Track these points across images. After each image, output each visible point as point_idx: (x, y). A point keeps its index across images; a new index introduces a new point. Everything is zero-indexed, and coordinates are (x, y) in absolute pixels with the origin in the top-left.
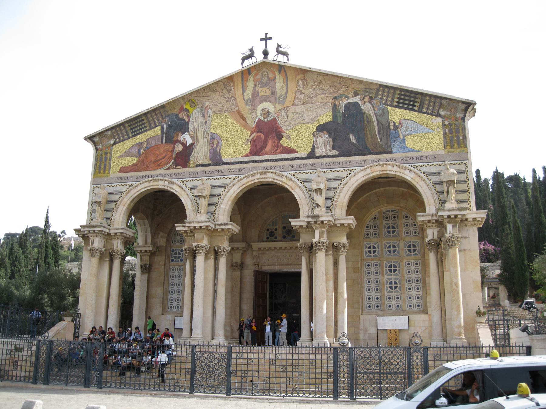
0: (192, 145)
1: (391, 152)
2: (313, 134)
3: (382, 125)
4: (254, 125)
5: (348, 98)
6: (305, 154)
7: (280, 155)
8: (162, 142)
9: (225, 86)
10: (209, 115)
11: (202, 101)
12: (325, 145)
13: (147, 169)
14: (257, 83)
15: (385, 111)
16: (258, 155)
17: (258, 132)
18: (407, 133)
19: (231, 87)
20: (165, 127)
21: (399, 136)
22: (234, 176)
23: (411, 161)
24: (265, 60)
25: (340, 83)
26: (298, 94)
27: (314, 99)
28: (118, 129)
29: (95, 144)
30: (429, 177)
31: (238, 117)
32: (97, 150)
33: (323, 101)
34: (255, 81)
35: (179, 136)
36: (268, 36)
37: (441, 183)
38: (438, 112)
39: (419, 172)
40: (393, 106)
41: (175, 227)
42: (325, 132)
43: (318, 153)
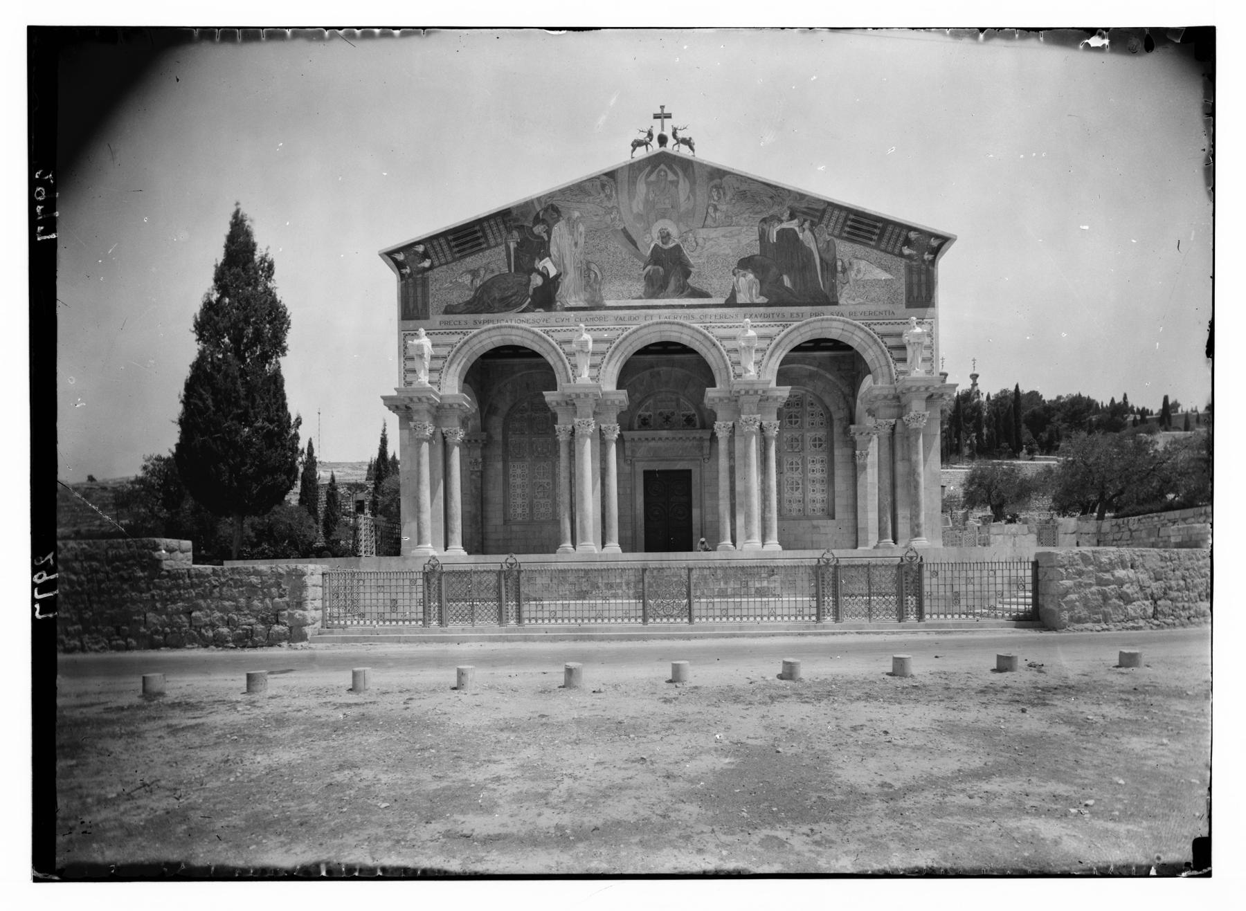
0: (557, 276)
1: (836, 303)
2: (733, 271)
3: (827, 264)
4: (649, 252)
5: (782, 221)
6: (722, 301)
7: (687, 299)
8: (510, 270)
9: (603, 186)
10: (581, 235)
11: (569, 208)
12: (750, 288)
13: (490, 310)
14: (651, 189)
15: (831, 245)
16: (657, 298)
17: (655, 264)
18: (859, 277)
19: (611, 191)
20: (512, 245)
21: (848, 282)
22: (623, 327)
23: (862, 317)
24: (663, 149)
25: (771, 198)
26: (711, 210)
27: (734, 218)
28: (435, 243)
29: (399, 266)
30: (885, 339)
31: (625, 240)
32: (402, 276)
33: (746, 224)
34: (648, 184)
35: (537, 262)
36: (666, 111)
37: (903, 348)
38: (901, 250)
39: (872, 332)
40: (843, 238)
41: (543, 396)
42: (750, 270)
43: (741, 298)
